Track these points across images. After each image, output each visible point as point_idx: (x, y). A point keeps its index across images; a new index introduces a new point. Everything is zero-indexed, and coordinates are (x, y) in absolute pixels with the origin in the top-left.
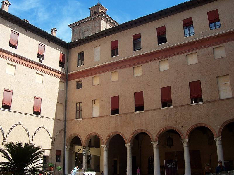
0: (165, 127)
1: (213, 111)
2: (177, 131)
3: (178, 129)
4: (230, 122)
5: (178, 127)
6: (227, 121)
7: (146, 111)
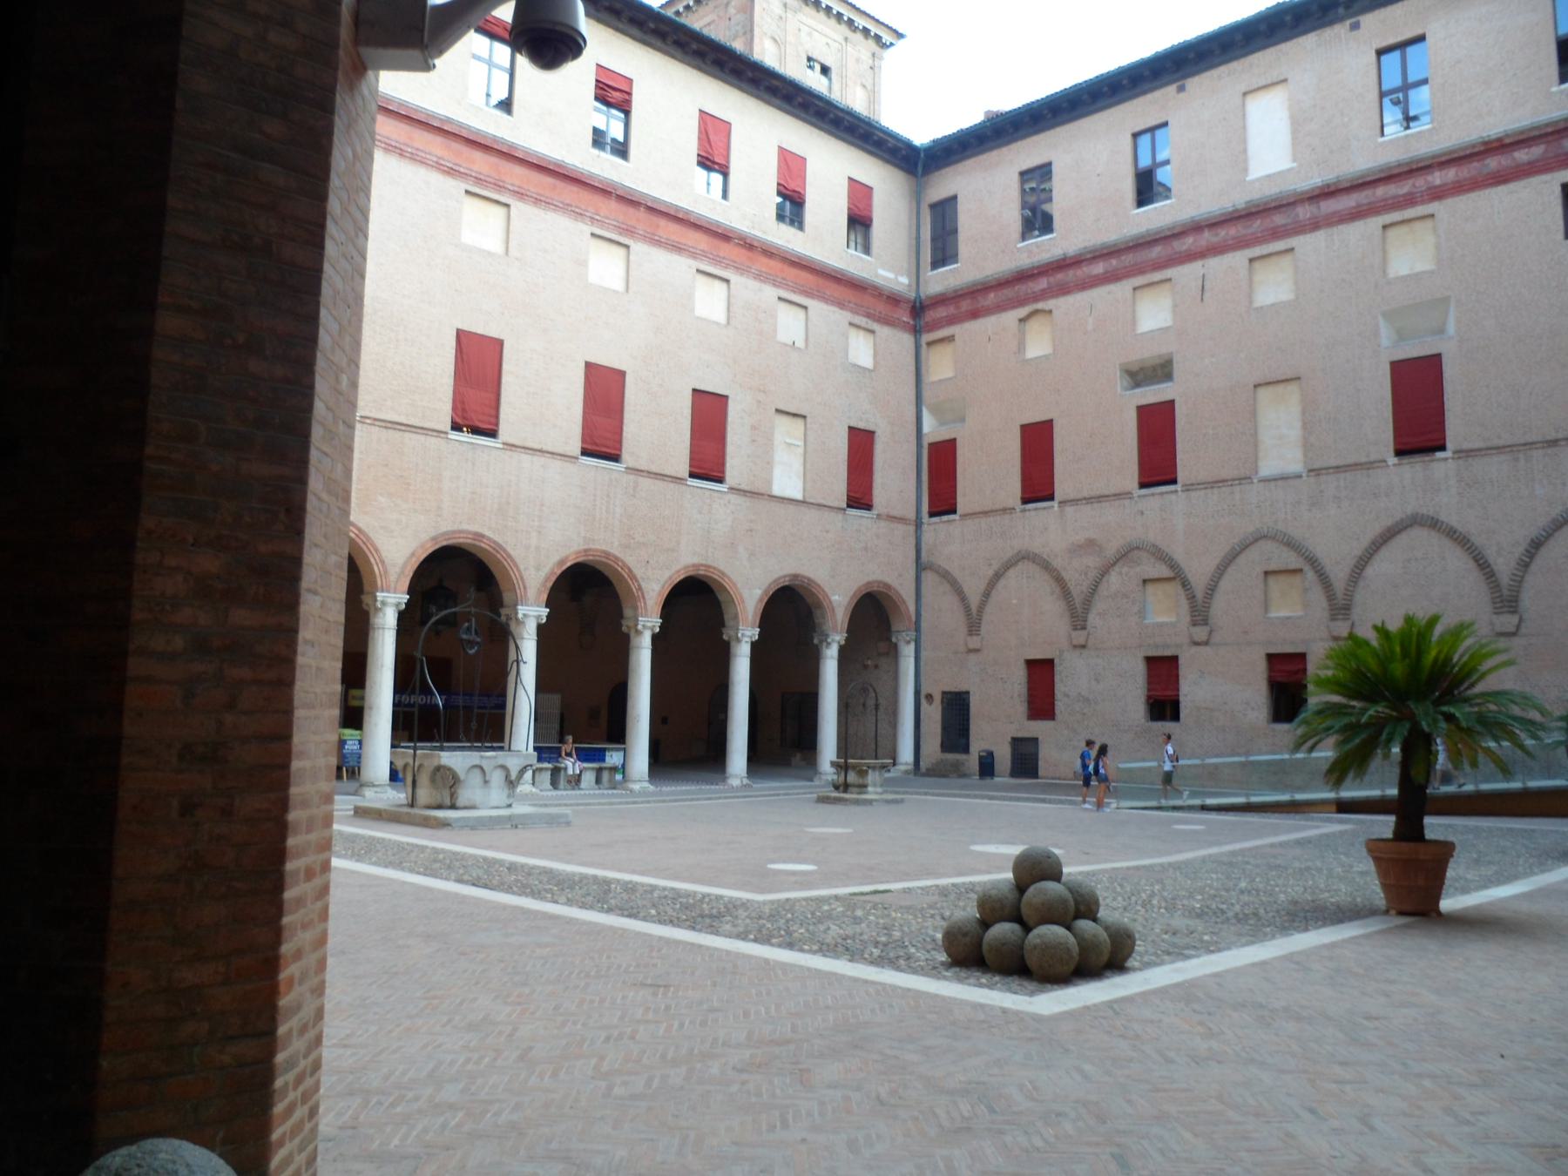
0: (586, 551)
1: (751, 531)
2: (626, 576)
5: (630, 560)
7: (510, 446)
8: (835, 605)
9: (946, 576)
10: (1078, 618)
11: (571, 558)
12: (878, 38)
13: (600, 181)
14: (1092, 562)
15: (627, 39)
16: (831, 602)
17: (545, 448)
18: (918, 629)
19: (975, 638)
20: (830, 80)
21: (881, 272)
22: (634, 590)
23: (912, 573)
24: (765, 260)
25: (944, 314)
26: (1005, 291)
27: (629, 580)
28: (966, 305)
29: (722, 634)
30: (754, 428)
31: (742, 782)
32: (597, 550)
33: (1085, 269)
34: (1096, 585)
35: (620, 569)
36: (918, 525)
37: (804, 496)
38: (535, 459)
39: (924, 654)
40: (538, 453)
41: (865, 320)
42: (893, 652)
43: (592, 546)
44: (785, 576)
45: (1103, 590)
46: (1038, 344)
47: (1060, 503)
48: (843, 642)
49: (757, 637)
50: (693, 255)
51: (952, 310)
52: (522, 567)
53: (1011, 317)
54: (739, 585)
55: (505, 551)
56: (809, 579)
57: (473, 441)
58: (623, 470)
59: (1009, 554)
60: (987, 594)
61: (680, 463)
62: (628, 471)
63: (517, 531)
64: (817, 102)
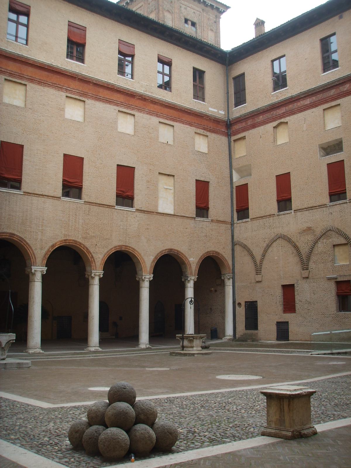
0: (65, 240)
1: (148, 229)
2: (85, 252)
3: (87, 249)
4: (167, 253)
5: (87, 244)
6: (163, 251)
7: (27, 193)
8: (191, 262)
9: (245, 247)
10: (305, 265)
11: (58, 244)
12: (217, 9)
13: (70, 73)
14: (310, 238)
15: (83, 10)
16: (189, 261)
17: (44, 194)
18: (233, 273)
19: (259, 275)
20: (196, 28)
21: (210, 109)
22: (90, 258)
23: (230, 247)
24: (152, 105)
25: (241, 127)
26: (267, 115)
27: (87, 253)
28: (250, 122)
29: (136, 277)
30: (148, 182)
31: (146, 346)
32: (71, 240)
33: (301, 102)
34: (313, 248)
35: (82, 248)
36: (232, 224)
37: (174, 213)
38: (39, 198)
39: (236, 284)
40: (41, 196)
41: (202, 131)
42: (222, 284)
43: (68, 238)
44: (166, 250)
45: (315, 251)
46: (283, 137)
47: (294, 211)
48: (196, 280)
49: (152, 279)
50: (117, 105)
51: (244, 124)
52: (33, 248)
53: (270, 126)
54: (142, 255)
55: (25, 241)
56: (178, 251)
57: (9, 191)
58: (83, 202)
59: (273, 236)
60: (264, 256)
61: (111, 198)
62: (85, 203)
63: (31, 232)
64: (176, 34)
